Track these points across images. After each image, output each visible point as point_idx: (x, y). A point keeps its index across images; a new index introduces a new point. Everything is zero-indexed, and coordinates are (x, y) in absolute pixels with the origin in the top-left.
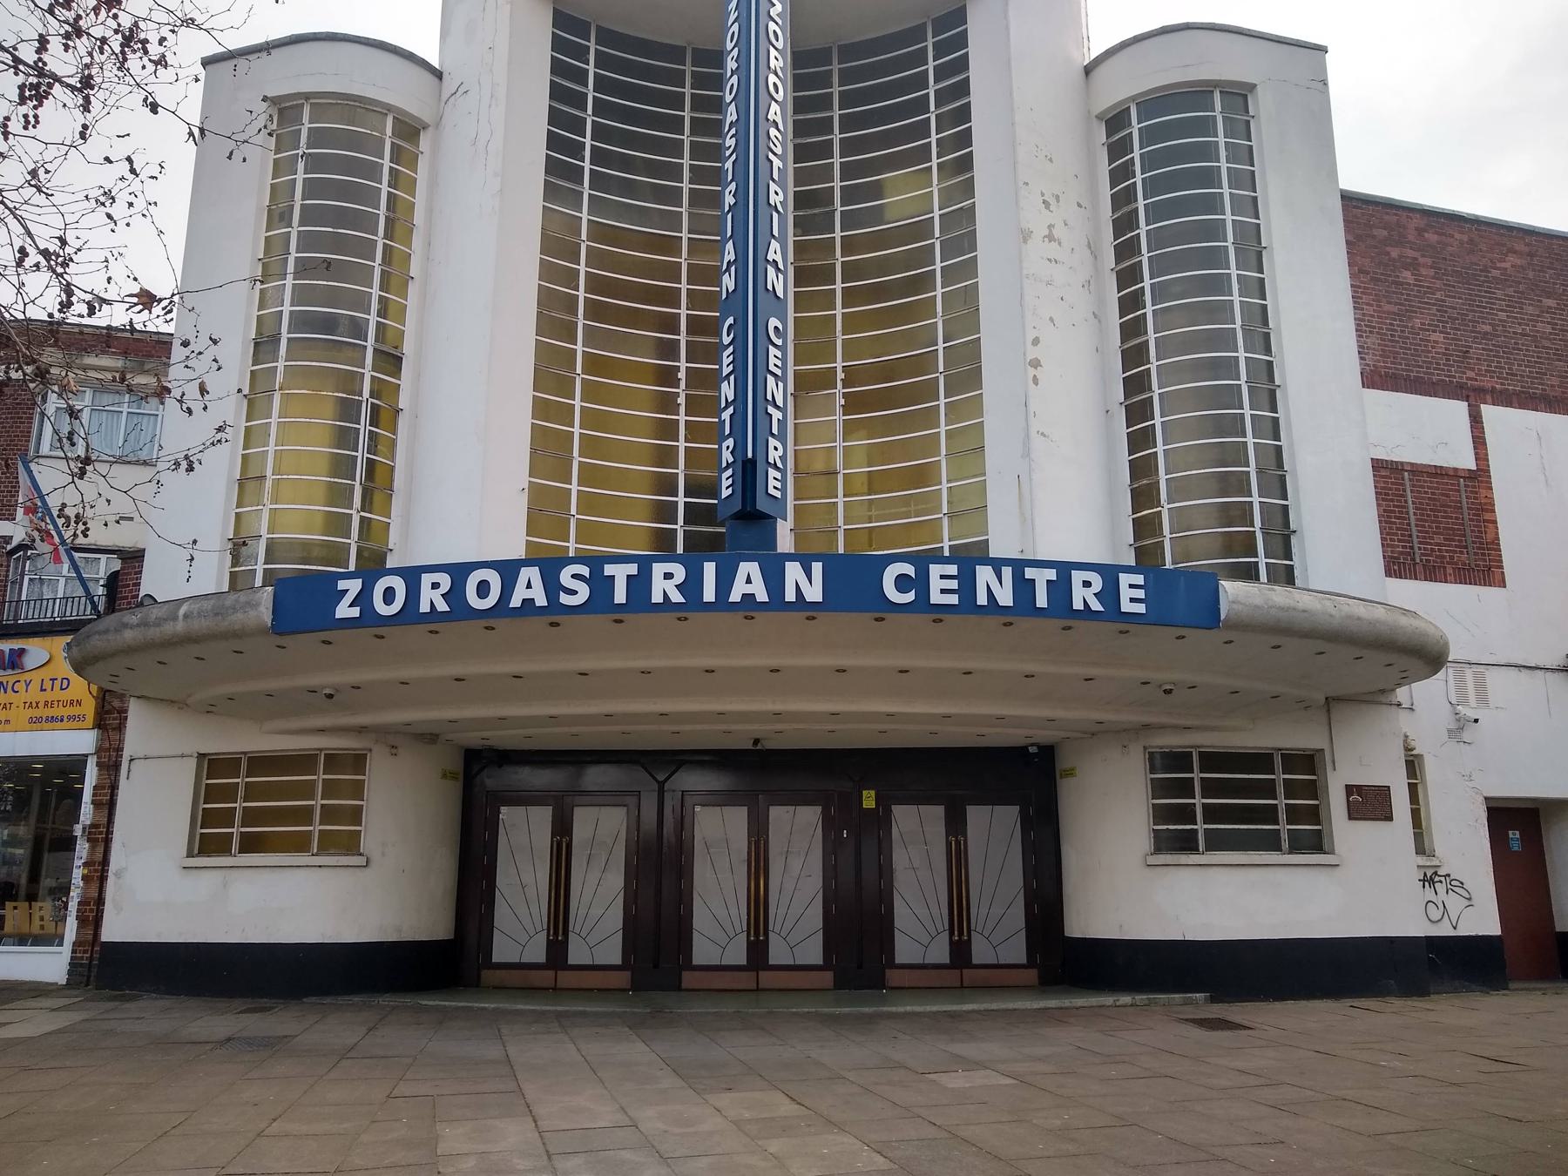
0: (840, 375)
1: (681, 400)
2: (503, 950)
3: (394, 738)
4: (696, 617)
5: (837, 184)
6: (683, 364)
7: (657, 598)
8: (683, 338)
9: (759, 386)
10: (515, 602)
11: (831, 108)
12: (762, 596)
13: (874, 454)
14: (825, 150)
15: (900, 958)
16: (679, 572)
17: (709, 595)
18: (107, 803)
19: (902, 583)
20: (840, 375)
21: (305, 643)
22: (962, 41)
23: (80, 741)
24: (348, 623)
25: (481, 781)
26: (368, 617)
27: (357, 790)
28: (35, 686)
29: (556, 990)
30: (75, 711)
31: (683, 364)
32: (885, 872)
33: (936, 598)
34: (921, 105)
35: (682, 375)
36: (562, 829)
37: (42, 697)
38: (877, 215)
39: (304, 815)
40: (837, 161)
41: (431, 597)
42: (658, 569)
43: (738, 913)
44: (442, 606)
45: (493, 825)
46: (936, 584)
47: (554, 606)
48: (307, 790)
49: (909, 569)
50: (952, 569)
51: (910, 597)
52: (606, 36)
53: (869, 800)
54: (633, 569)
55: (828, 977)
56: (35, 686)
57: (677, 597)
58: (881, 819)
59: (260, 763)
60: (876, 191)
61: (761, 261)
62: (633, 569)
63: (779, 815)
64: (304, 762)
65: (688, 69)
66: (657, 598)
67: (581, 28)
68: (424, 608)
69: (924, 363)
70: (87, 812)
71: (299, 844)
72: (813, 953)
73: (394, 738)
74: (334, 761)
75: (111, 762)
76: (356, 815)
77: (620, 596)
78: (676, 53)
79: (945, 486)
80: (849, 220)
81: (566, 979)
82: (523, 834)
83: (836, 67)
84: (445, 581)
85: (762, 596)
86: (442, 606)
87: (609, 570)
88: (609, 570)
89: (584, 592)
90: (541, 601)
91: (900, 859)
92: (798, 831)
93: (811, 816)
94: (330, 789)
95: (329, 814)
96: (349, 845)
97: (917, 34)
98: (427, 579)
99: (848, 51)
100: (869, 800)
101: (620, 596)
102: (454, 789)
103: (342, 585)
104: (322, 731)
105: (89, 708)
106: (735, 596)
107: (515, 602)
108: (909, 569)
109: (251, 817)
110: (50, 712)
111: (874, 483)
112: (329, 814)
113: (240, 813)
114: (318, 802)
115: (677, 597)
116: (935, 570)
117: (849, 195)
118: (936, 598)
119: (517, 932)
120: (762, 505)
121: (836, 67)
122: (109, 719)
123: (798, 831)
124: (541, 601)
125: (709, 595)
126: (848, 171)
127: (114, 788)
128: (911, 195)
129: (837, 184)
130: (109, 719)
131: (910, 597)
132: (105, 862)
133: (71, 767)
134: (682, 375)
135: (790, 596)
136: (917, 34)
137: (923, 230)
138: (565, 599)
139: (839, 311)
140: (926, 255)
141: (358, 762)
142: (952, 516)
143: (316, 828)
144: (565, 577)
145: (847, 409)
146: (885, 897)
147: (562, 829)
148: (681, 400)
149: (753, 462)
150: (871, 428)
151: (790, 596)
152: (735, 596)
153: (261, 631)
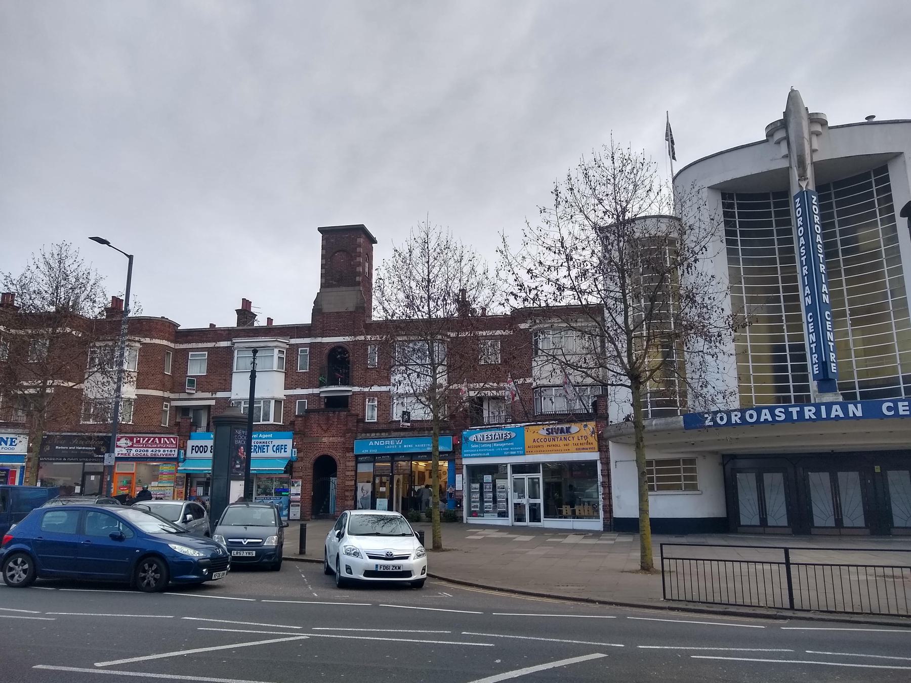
0: (848, 312)
1: (785, 327)
2: (744, 521)
3: (704, 454)
4: (819, 422)
5: (838, 238)
6: (784, 314)
7: (807, 417)
8: (782, 304)
9: (825, 336)
10: (762, 420)
11: (832, 208)
12: (842, 415)
13: (866, 342)
14: (832, 225)
15: (896, 525)
16: (813, 409)
17: (824, 416)
18: (607, 474)
19: (889, 409)
20: (848, 312)
21: (695, 431)
22: (887, 179)
23: (594, 456)
24: (710, 426)
25: (730, 466)
26: (716, 424)
27: (693, 470)
28: (576, 439)
29: (764, 534)
30: (591, 446)
31: (784, 314)
32: (887, 494)
33: (901, 413)
34: (872, 205)
35: (784, 318)
36: (760, 481)
37: (579, 442)
38: (856, 250)
39: (679, 478)
40: (837, 229)
41: (735, 419)
42: (806, 409)
43: (829, 509)
44: (739, 421)
45: (735, 480)
46: (901, 409)
47: (774, 421)
48: (678, 471)
49: (891, 404)
50: (906, 403)
51: (892, 413)
52: (740, 196)
53: (877, 469)
54: (798, 409)
55: (868, 531)
56: (576, 439)
57: (813, 417)
58: (883, 475)
59: (659, 462)
60: (854, 230)
61: (820, 294)
62: (798, 409)
63: (839, 474)
64: (676, 462)
65: (772, 201)
66: (807, 417)
67: (731, 196)
68: (733, 422)
69: (884, 306)
70: (600, 478)
71: (678, 487)
72: (861, 522)
73: (704, 454)
74: (686, 461)
75: (606, 462)
76: (693, 478)
77: (795, 417)
78: (765, 196)
79: (897, 353)
80: (845, 252)
81: (768, 530)
82: (746, 483)
83: (833, 191)
84: (739, 415)
85: (842, 415)
86: (739, 421)
87: (790, 409)
88: (790, 409)
89: (783, 417)
90: (770, 419)
91: (892, 490)
92: (850, 482)
93: (854, 476)
94: (685, 470)
95: (686, 478)
96: (694, 487)
97: (867, 176)
98: (733, 414)
99: (837, 184)
100: (877, 469)
101: (795, 417)
102: (721, 467)
103: (706, 416)
104: (686, 452)
105: (595, 444)
106: (833, 416)
107: (762, 420)
108: (891, 404)
109: (659, 479)
110: (582, 447)
111: (867, 352)
112: (686, 478)
113: (653, 477)
114: (682, 474)
115: (813, 417)
116: (900, 404)
117: (844, 243)
118: (901, 413)
119: (748, 514)
120: (830, 376)
121: (833, 191)
122: (603, 449)
123: (850, 482)
124: (770, 419)
125: (824, 416)
126: (842, 233)
127: (609, 470)
128: (872, 235)
129: (838, 238)
130: (603, 449)
131: (892, 413)
132: (610, 493)
133: (593, 464)
134: (784, 318)
135: (851, 415)
136: (867, 176)
137: (877, 255)
138: (777, 418)
139: (843, 278)
140: (880, 265)
141: (692, 461)
142: (901, 365)
143: (683, 482)
144: (777, 412)
145: (852, 325)
146: (888, 503)
147: (760, 481)
148: (785, 327)
149: (826, 362)
150: (864, 332)
151: (851, 415)
152: (833, 416)
153: (681, 429)
